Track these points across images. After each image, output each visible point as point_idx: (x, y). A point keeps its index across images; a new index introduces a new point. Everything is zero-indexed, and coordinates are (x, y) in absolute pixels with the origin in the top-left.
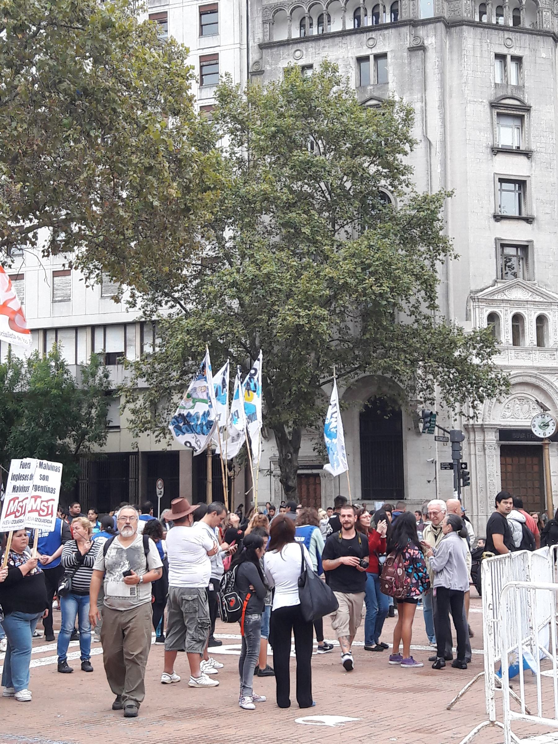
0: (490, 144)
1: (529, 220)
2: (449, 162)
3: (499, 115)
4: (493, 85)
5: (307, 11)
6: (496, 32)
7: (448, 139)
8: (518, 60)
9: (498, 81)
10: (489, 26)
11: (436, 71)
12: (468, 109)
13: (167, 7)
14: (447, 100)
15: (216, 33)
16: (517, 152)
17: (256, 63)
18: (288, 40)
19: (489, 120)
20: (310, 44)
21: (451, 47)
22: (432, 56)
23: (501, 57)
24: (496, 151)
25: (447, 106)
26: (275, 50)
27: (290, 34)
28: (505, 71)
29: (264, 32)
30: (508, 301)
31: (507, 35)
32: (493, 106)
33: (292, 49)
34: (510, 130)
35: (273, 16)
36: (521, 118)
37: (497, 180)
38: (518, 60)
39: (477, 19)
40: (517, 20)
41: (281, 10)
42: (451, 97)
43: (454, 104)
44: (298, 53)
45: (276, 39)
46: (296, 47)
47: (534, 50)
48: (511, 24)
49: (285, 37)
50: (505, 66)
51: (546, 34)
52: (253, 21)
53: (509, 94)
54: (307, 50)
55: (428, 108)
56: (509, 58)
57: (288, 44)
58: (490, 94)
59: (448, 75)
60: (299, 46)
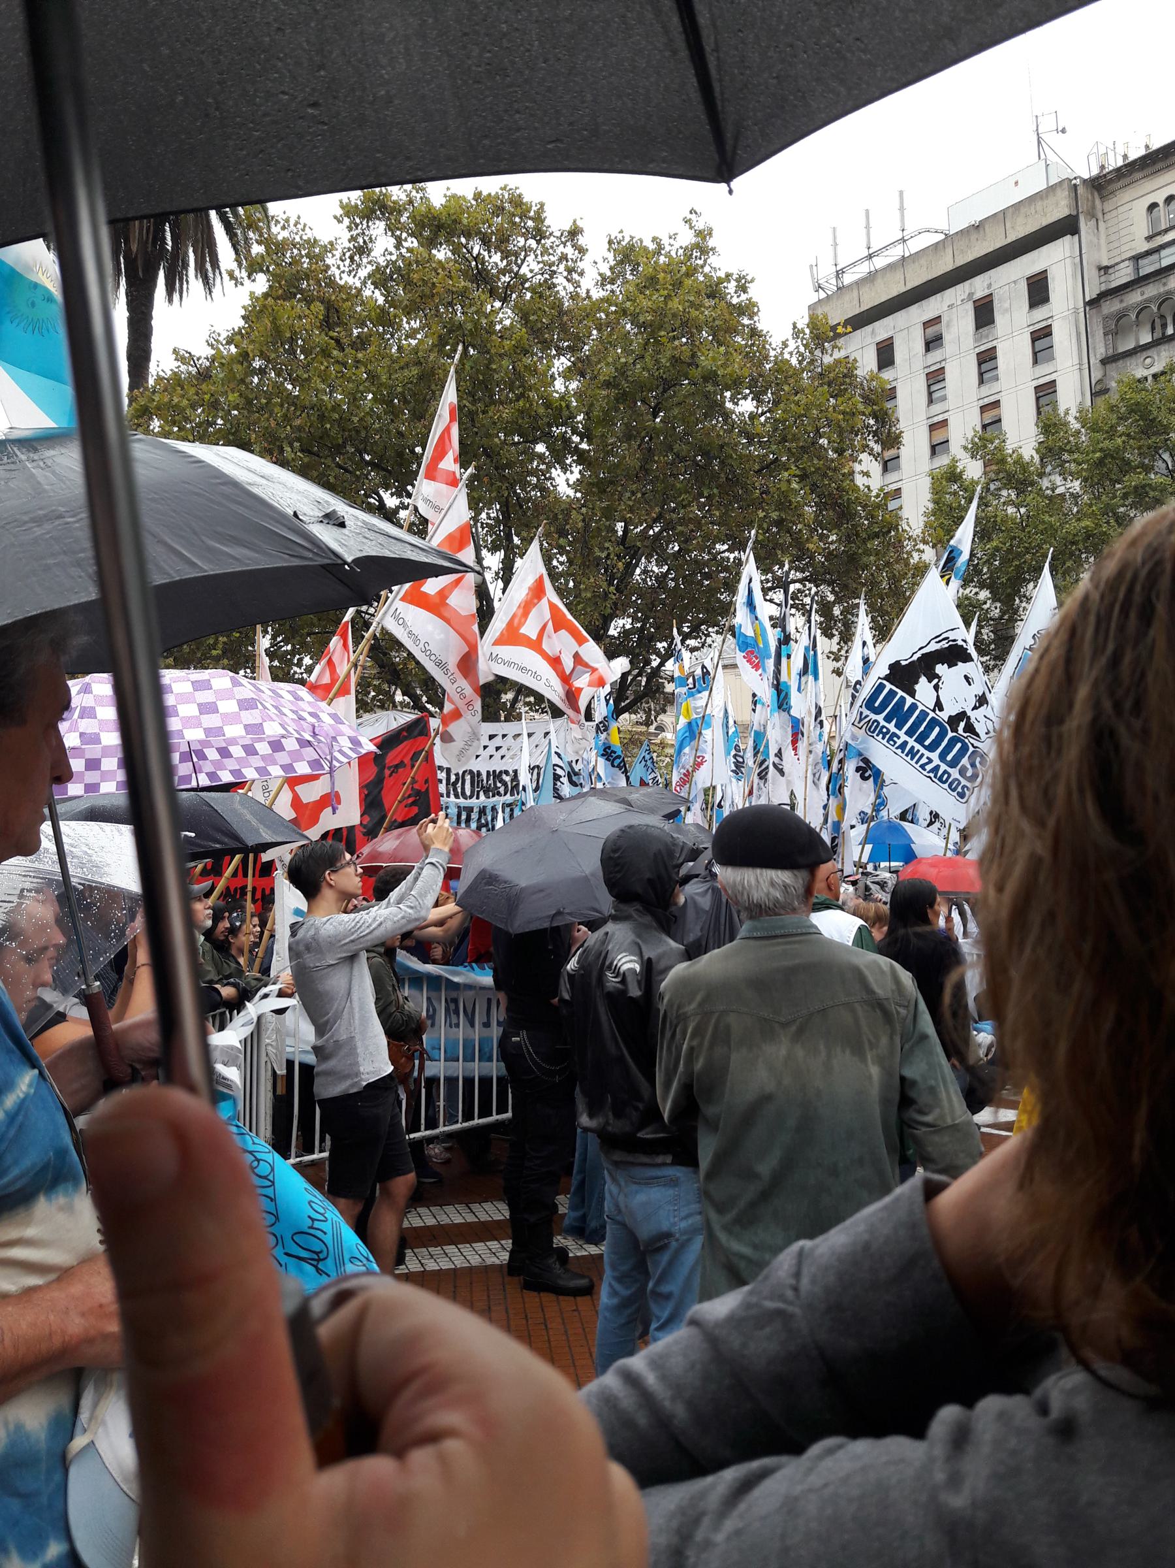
5: (1155, 309)
13: (995, 342)
15: (1052, 358)
17: (1099, 382)
18: (1134, 349)
20: (1162, 347)
26: (1120, 363)
27: (1137, 340)
29: (1106, 345)
33: (1141, 357)
35: (1116, 325)
41: (1125, 315)
44: (1148, 361)
45: (1121, 350)
46: (1145, 354)
49: (1131, 345)
52: (1093, 336)
54: (1159, 355)
57: (1136, 353)
60: (1149, 353)
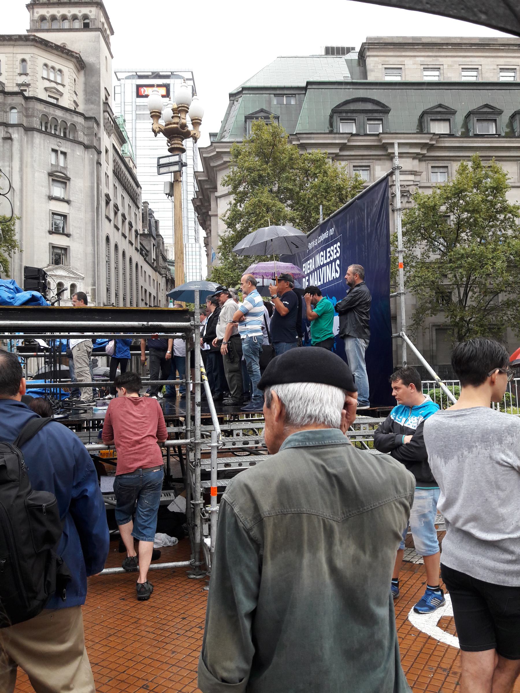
0: (48, 194)
1: (68, 235)
2: (24, 201)
3: (53, 180)
4: (50, 164)
6: (53, 138)
7: (24, 188)
8: (64, 154)
9: (53, 162)
10: (50, 134)
11: (18, 152)
12: (36, 175)
14: (24, 169)
16: (63, 200)
19: (47, 182)
21: (27, 141)
22: (16, 145)
23: (55, 151)
24: (51, 198)
25: (24, 172)
28: (57, 158)
30: (55, 276)
31: (58, 140)
32: (50, 174)
34: (59, 189)
36: (65, 183)
37: (51, 213)
38: (64, 154)
39: (43, 129)
40: (65, 133)
42: (26, 167)
43: (28, 171)
47: (73, 150)
48: (62, 135)
50: (57, 155)
51: (80, 143)
53: (59, 170)
55: (13, 170)
56: (59, 152)
58: (49, 169)
59: (25, 155)
